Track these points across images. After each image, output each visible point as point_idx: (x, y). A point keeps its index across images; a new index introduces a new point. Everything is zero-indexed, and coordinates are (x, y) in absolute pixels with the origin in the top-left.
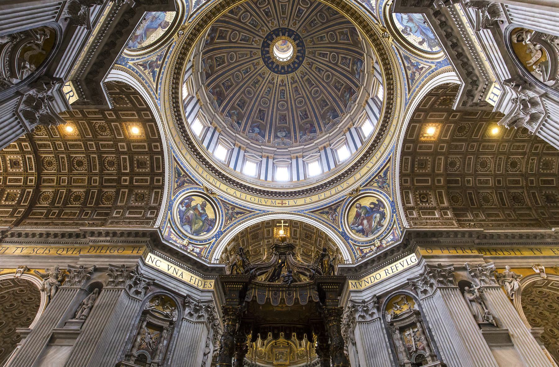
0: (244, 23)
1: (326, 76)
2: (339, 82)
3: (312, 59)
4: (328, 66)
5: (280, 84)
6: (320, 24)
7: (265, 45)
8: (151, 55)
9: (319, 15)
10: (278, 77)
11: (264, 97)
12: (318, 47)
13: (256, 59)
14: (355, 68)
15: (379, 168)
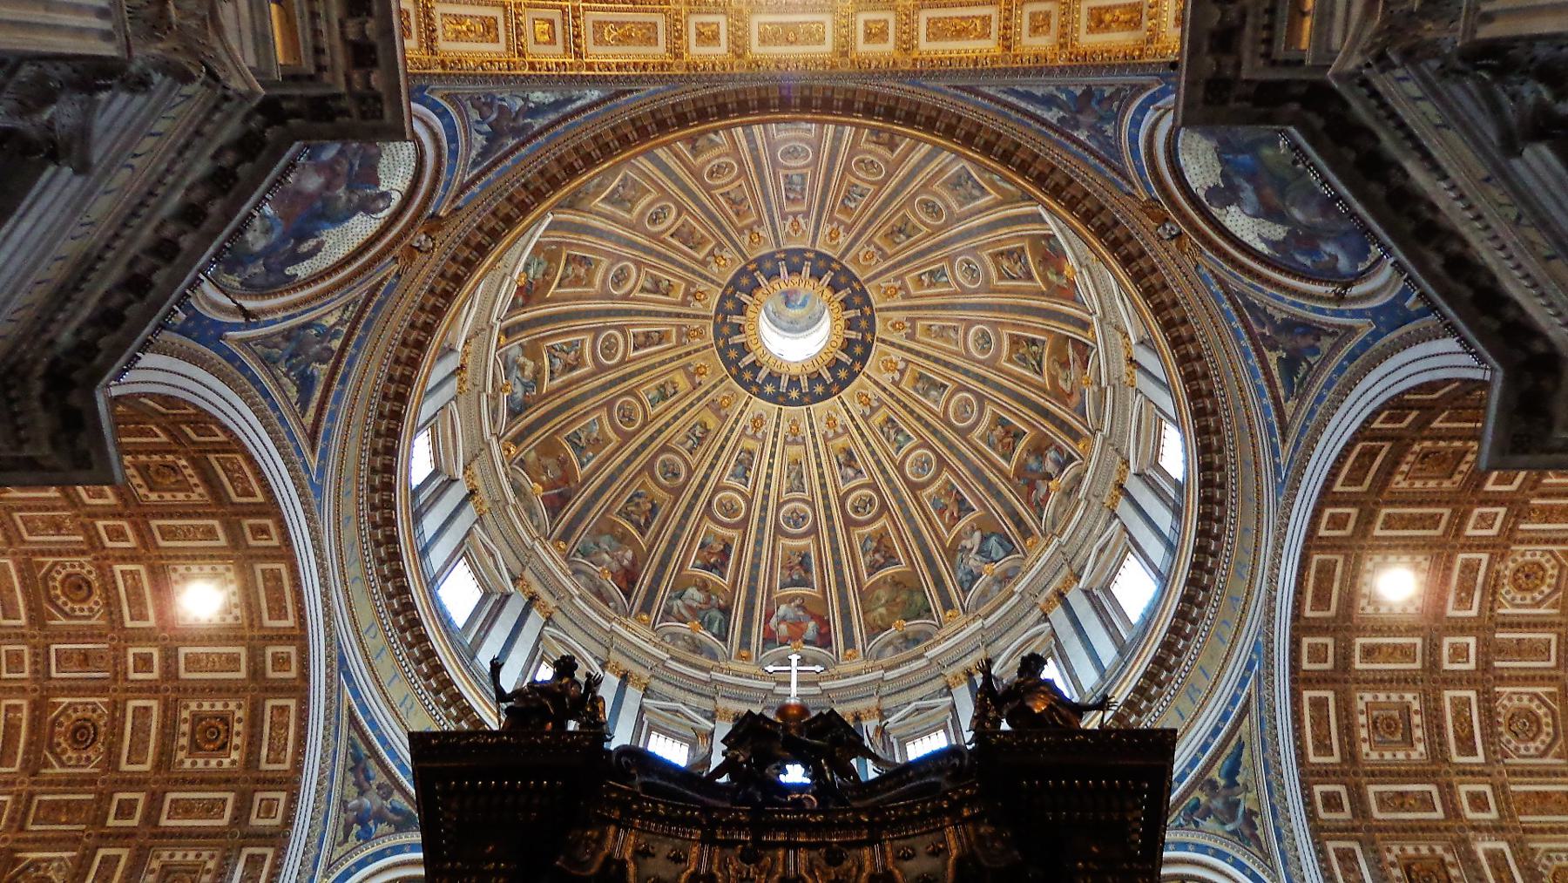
0: (926, 445)
1: (627, 278)
2: (577, 281)
3: (687, 316)
4: (628, 313)
5: (806, 215)
6: (672, 444)
7: (858, 350)
8: (1219, 854)
9: (676, 475)
10: (814, 242)
11: (872, 183)
12: (672, 360)
13: (896, 309)
14: (530, 365)
15: (344, 381)
